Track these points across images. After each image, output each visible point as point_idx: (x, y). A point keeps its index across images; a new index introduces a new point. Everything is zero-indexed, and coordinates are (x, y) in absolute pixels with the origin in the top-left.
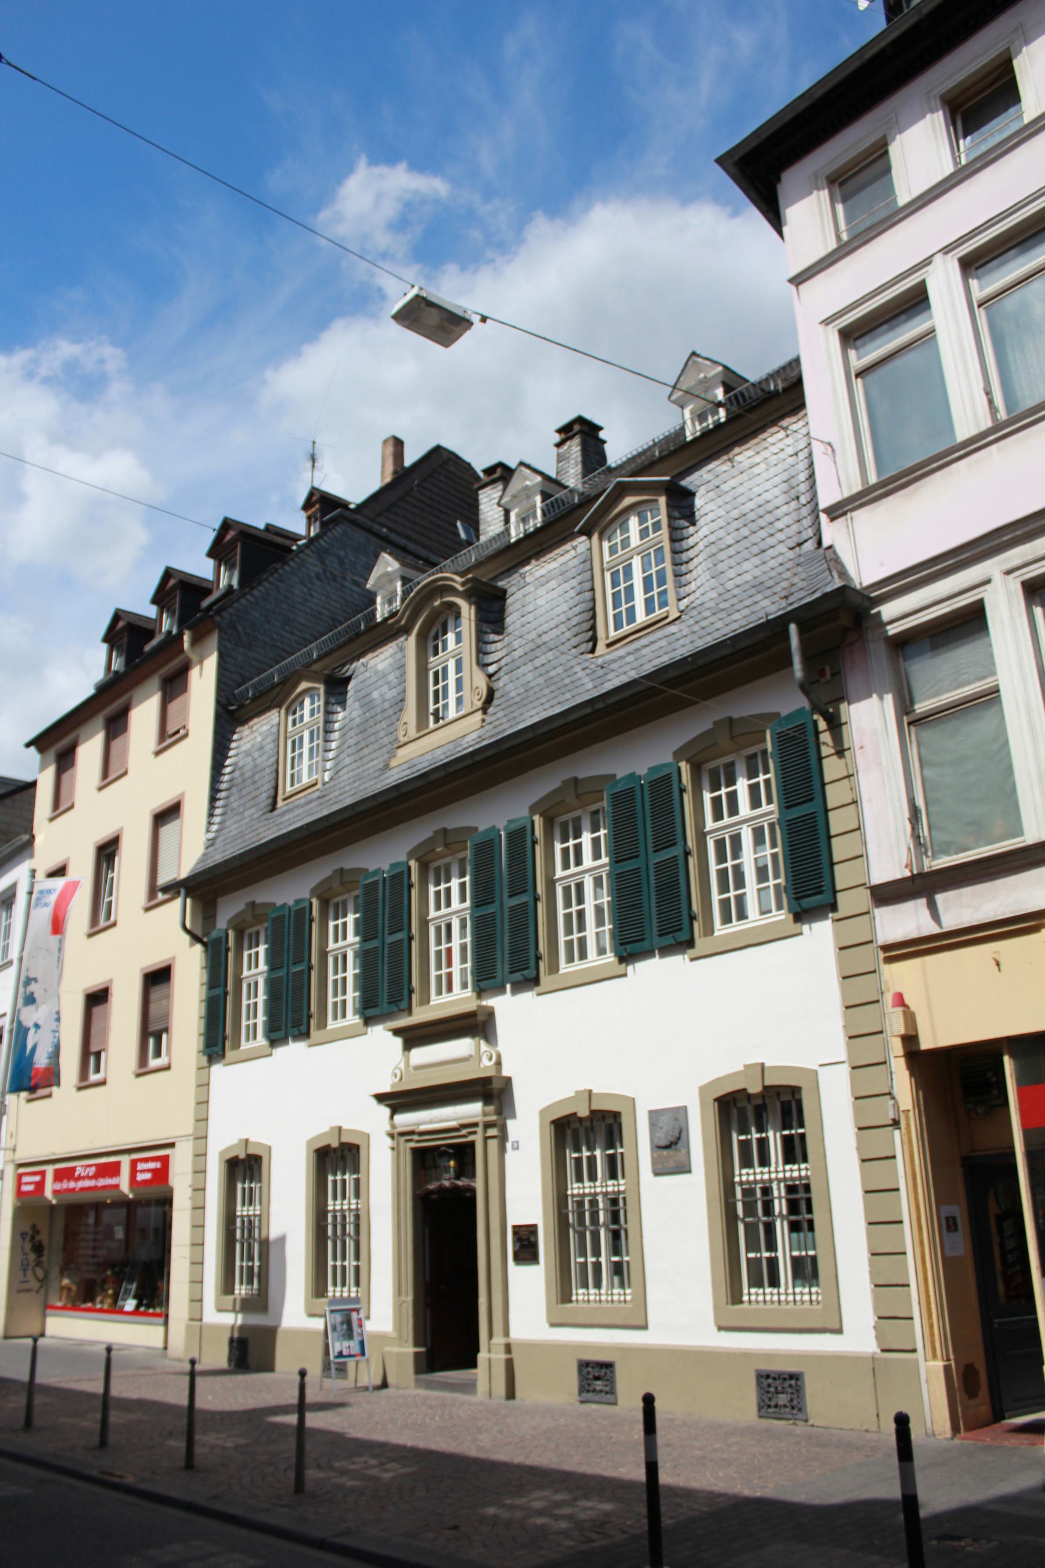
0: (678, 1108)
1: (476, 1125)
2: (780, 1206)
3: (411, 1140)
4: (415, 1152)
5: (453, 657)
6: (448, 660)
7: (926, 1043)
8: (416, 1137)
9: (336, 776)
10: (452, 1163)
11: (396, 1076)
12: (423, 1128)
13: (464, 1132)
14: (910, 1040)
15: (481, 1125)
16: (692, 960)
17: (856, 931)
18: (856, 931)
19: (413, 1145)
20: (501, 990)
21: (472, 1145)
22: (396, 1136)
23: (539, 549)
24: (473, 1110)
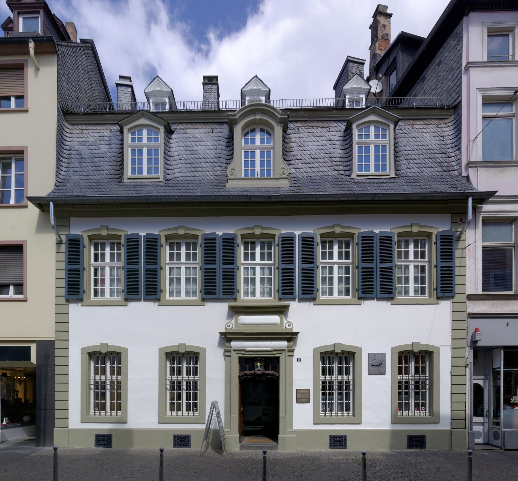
0: (382, 353)
1: (284, 350)
2: (412, 387)
3: (241, 353)
4: (240, 359)
5: (259, 149)
6: (256, 149)
7: (479, 344)
8: (243, 352)
9: (174, 179)
10: (258, 364)
11: (229, 326)
12: (248, 349)
13: (275, 353)
14: (474, 343)
15: (287, 351)
16: (392, 304)
17: (459, 307)
18: (459, 307)
19: (241, 355)
20: (294, 299)
21: (278, 358)
22: (232, 351)
23: (307, 119)
24: (283, 344)
